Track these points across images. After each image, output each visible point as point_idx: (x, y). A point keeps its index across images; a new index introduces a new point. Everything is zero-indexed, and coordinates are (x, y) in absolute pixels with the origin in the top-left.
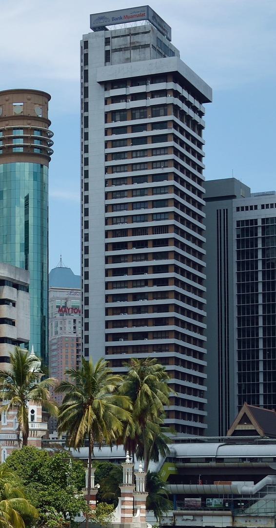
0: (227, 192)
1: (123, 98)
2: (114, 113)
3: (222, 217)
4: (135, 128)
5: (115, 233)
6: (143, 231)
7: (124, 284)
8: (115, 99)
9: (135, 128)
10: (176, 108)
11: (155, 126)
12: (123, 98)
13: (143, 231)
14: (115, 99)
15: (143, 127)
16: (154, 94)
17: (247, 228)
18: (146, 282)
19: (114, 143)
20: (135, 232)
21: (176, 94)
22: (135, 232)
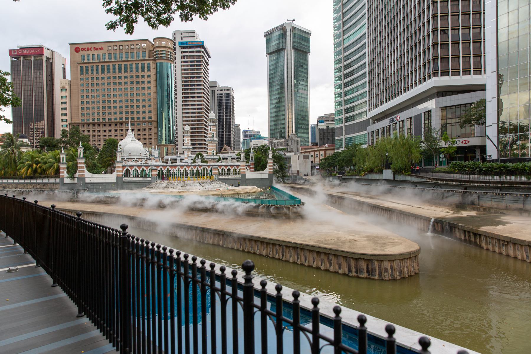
0: (214, 85)
1: (187, 52)
2: (184, 56)
3: (213, 92)
4: (191, 62)
5: (185, 93)
6: (194, 93)
7: (189, 109)
8: (184, 52)
9: (191, 62)
10: (203, 57)
11: (197, 61)
12: (187, 52)
13: (194, 93)
14: (184, 52)
15: (193, 62)
16: (197, 52)
17: (220, 96)
18: (195, 109)
19: (184, 66)
20: (191, 93)
21: (203, 52)
22: (191, 93)
